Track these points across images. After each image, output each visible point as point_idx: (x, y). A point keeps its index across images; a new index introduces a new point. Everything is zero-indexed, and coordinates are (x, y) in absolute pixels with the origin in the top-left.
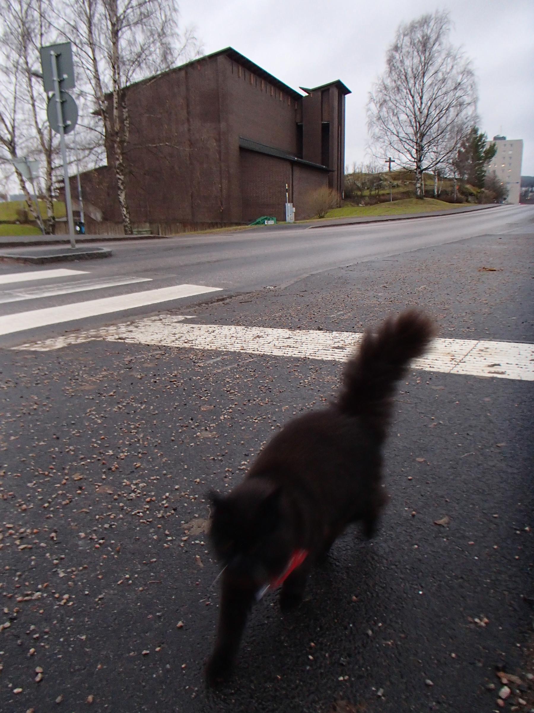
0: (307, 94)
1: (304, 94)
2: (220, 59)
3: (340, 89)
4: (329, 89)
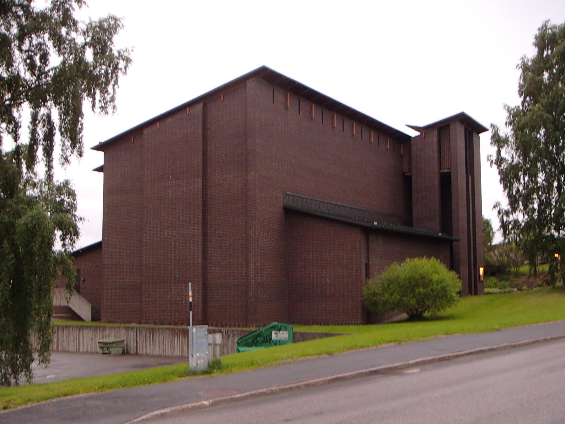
0: (417, 133)
1: (413, 134)
2: (251, 84)
3: (469, 127)
4: (448, 126)
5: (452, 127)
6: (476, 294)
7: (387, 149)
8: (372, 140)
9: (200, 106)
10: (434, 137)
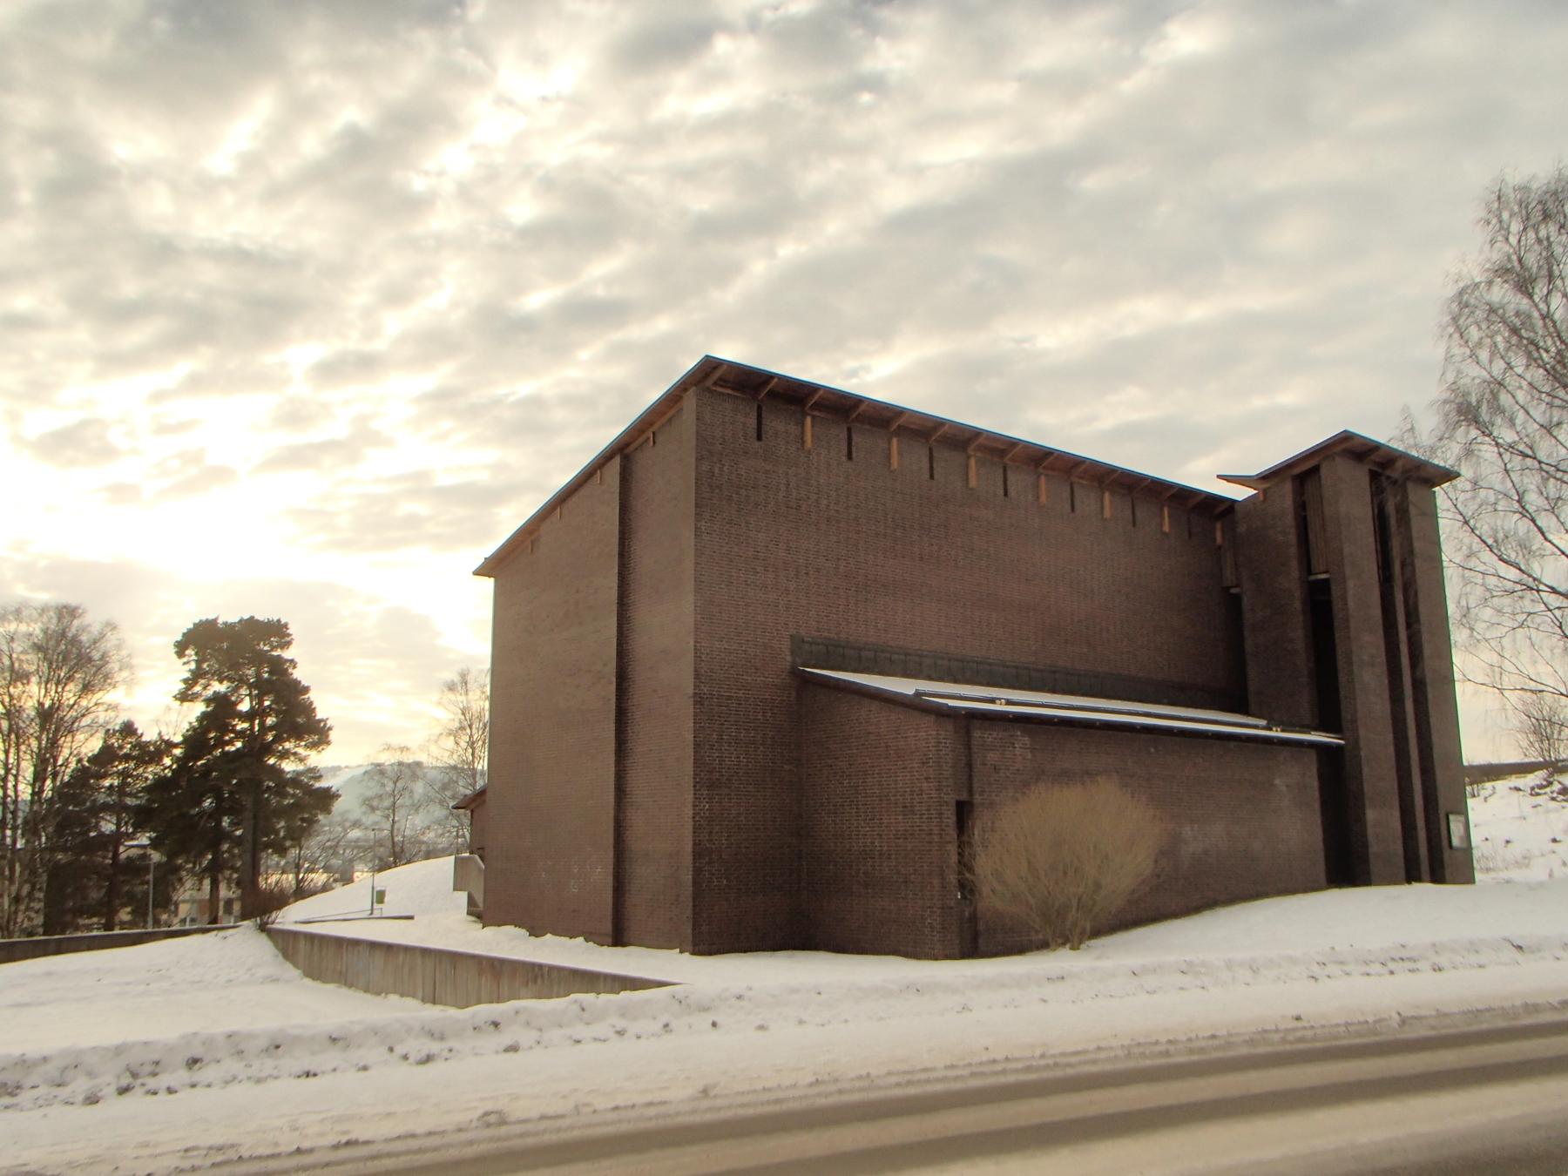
1: (1240, 493)
2: (690, 402)
4: (1315, 470)
5: (1324, 471)
6: (1438, 876)
7: (1164, 534)
8: (1107, 514)
9: (617, 460)
10: (1285, 496)
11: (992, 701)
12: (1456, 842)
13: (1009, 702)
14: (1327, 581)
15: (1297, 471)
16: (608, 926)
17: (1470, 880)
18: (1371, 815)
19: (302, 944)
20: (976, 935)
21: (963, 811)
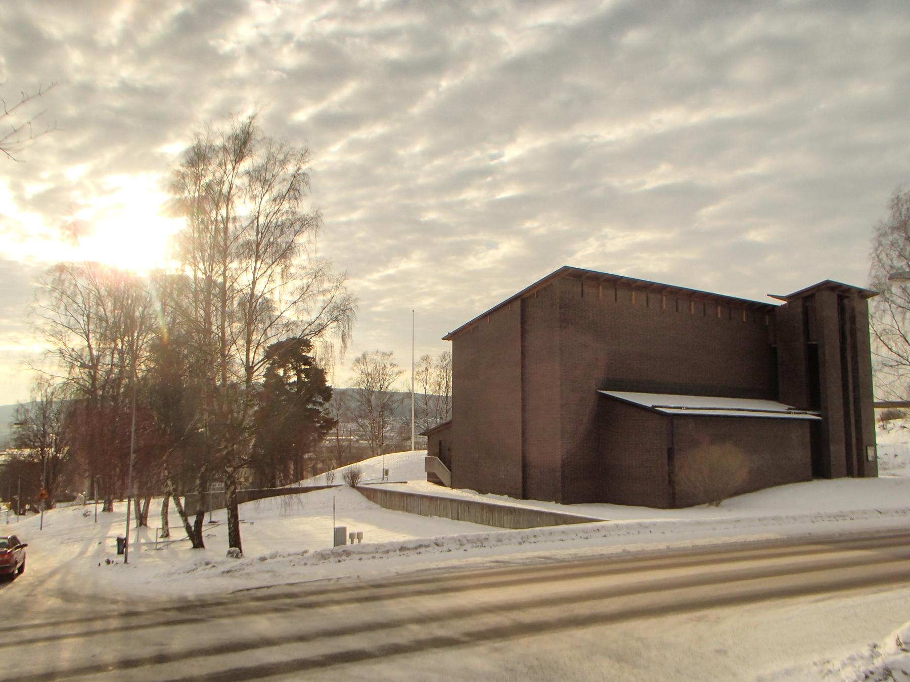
4: (813, 295)
6: (861, 474)
9: (519, 302)
11: (681, 408)
12: (870, 458)
13: (687, 408)
14: (816, 345)
15: (806, 294)
16: (520, 491)
17: (874, 474)
18: (832, 448)
19: (379, 494)
20: (673, 498)
21: (671, 453)
